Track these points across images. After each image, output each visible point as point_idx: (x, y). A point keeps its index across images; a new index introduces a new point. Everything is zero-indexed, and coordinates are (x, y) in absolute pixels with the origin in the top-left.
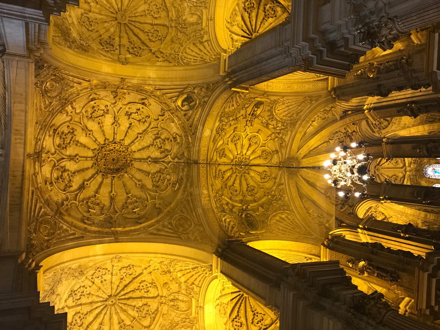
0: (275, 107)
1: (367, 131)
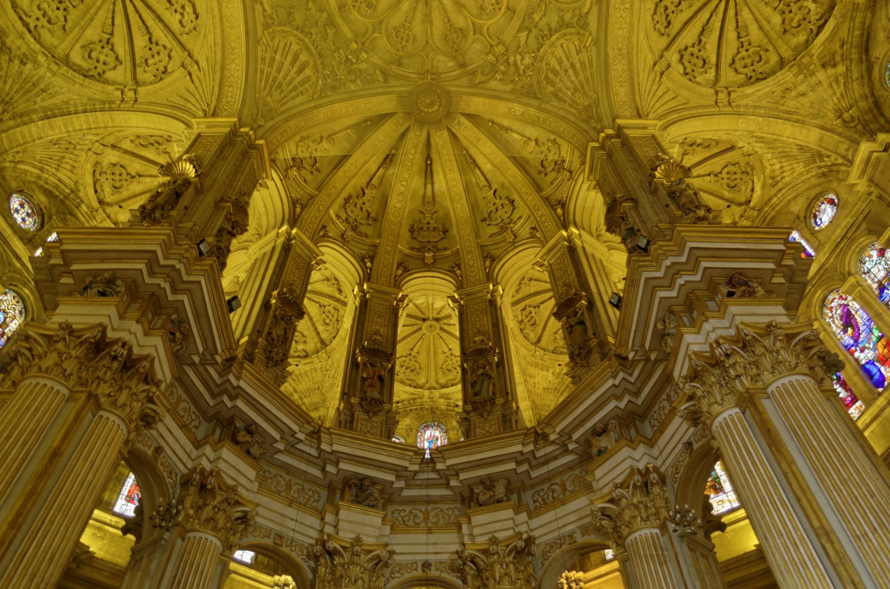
0: (571, 34)
1: (516, 266)
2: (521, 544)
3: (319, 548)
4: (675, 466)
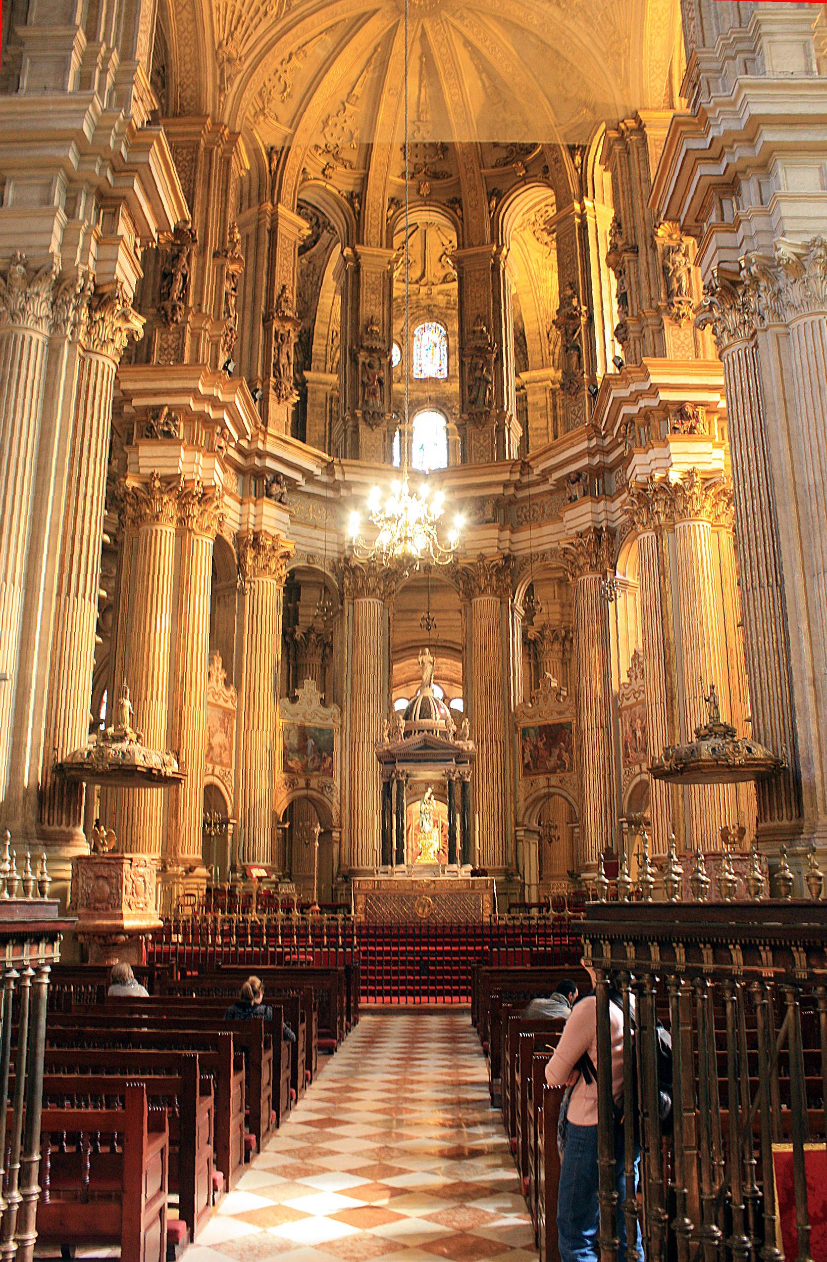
2: (502, 562)
3: (342, 565)
4: (622, 525)
